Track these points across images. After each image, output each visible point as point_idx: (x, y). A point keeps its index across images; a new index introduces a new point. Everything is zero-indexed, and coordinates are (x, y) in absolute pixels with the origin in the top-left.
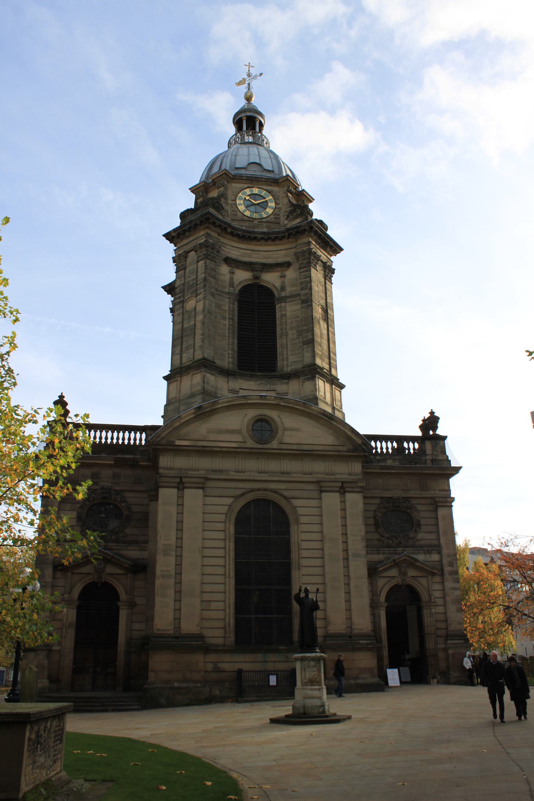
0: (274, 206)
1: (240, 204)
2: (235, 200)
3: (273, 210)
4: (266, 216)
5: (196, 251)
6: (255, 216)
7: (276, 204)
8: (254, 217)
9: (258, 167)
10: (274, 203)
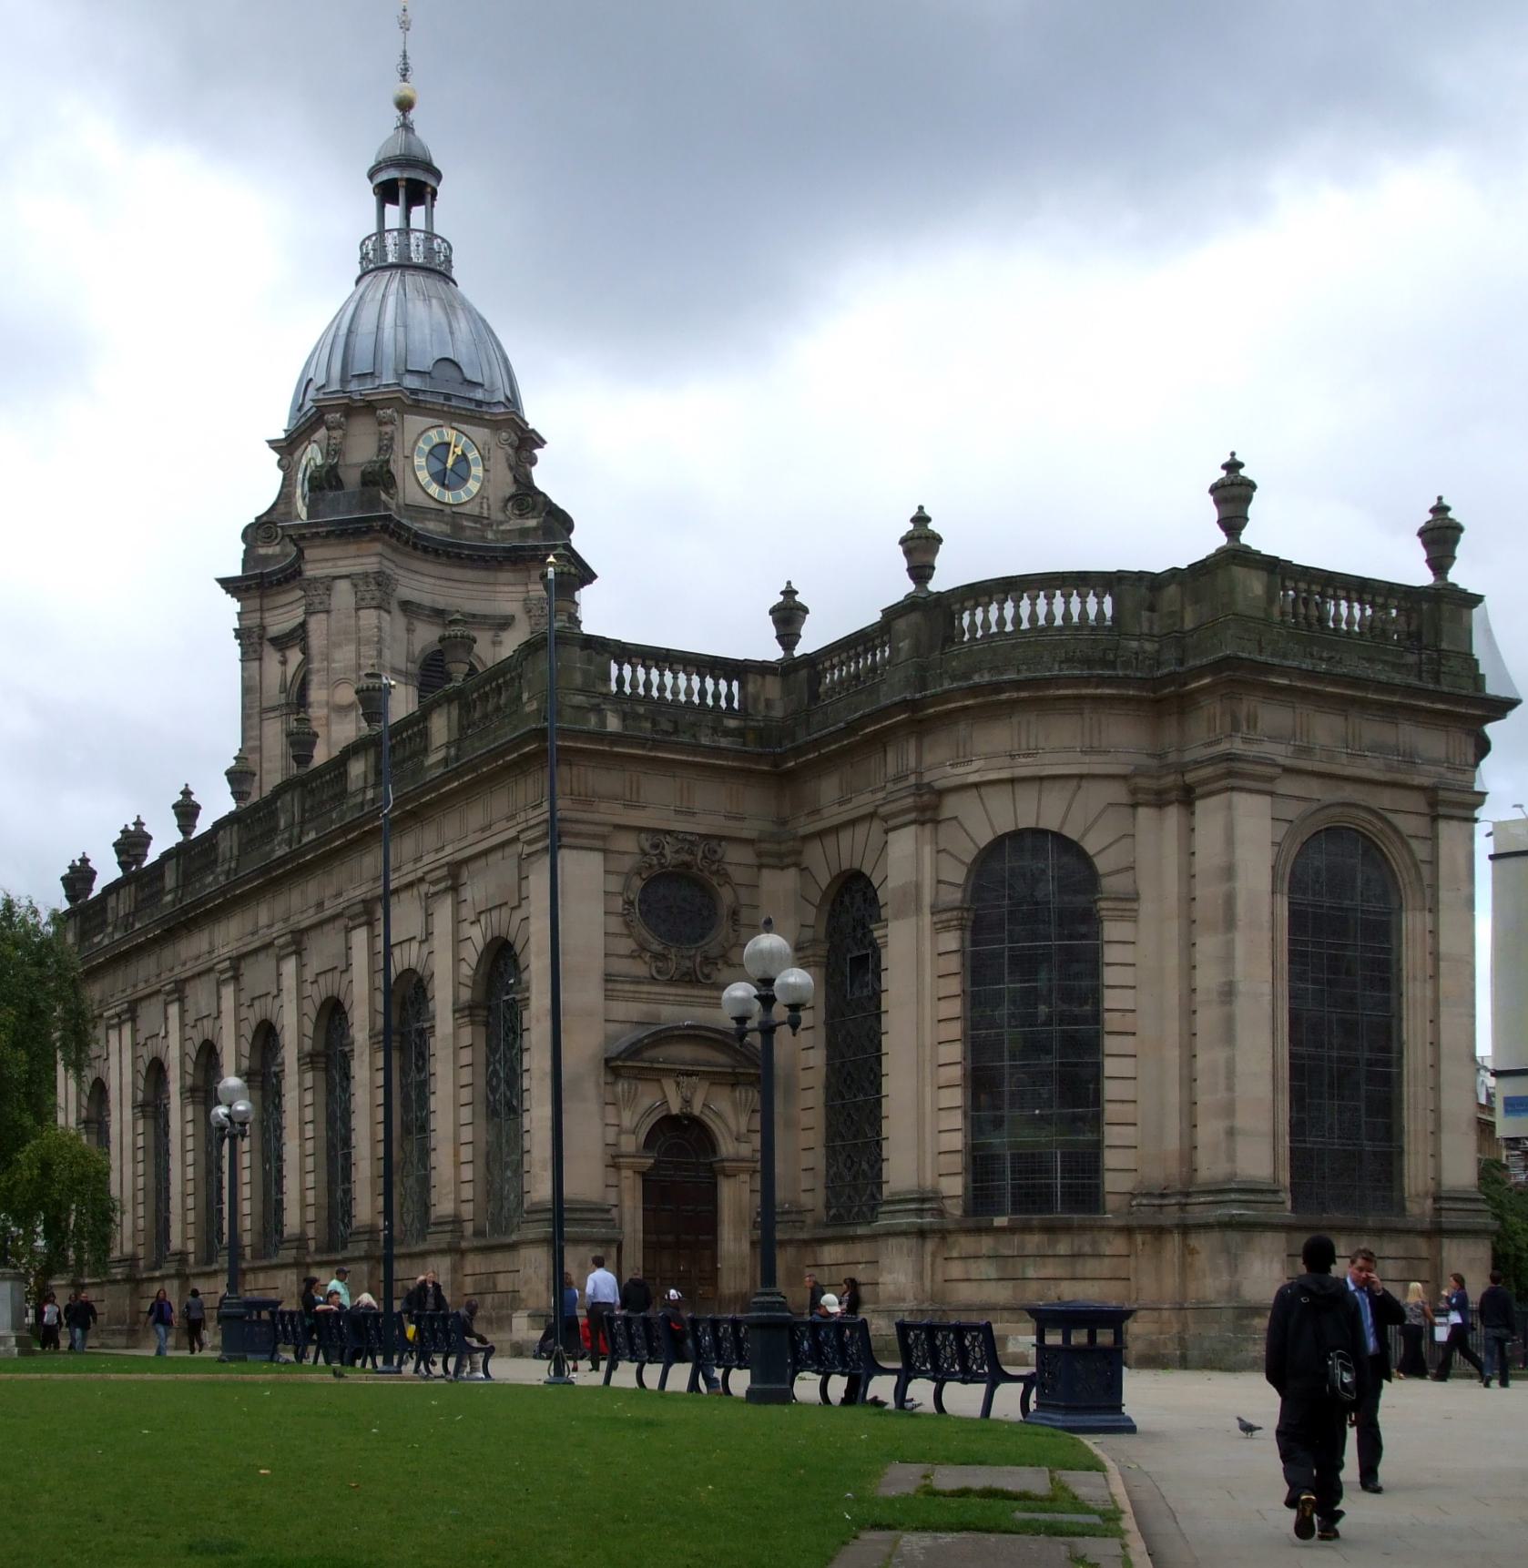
0: (481, 475)
1: (421, 468)
2: (409, 458)
3: (479, 485)
4: (467, 499)
5: (355, 586)
6: (448, 497)
7: (486, 470)
8: (446, 501)
9: (455, 374)
10: (481, 468)
